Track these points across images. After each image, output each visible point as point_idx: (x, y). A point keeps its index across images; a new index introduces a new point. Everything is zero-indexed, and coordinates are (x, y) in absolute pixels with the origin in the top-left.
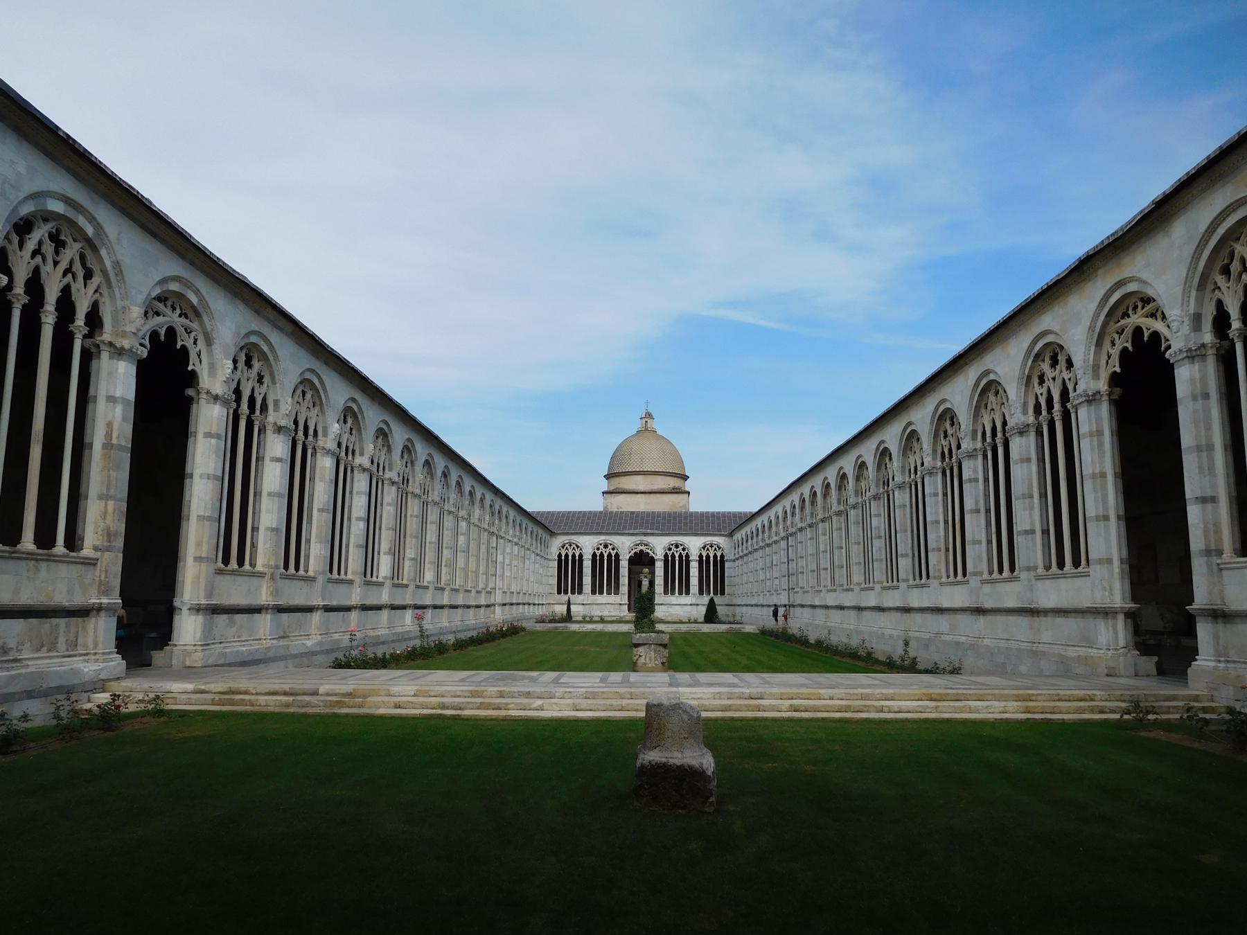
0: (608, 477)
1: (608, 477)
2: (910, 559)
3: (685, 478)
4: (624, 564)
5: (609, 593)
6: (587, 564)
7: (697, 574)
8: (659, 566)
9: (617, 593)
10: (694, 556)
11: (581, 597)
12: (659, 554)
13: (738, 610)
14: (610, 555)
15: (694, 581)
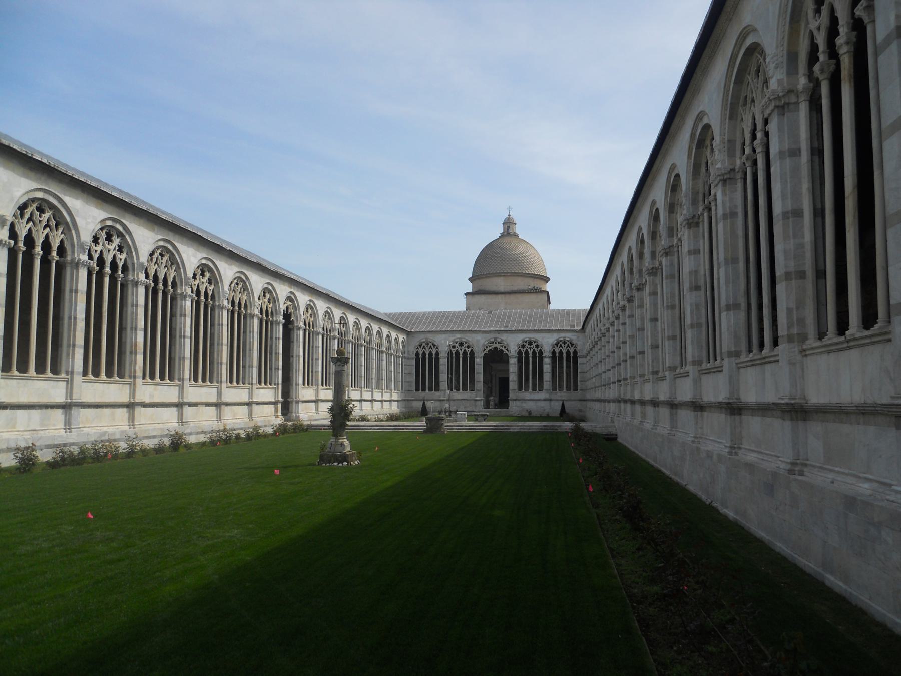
0: (471, 280)
1: (471, 280)
2: (742, 315)
3: (546, 280)
4: (479, 361)
5: (465, 389)
6: (443, 361)
7: (550, 370)
8: (513, 361)
9: (472, 389)
10: (547, 352)
11: (438, 393)
12: (513, 350)
13: (589, 404)
14: (465, 353)
15: (547, 376)
